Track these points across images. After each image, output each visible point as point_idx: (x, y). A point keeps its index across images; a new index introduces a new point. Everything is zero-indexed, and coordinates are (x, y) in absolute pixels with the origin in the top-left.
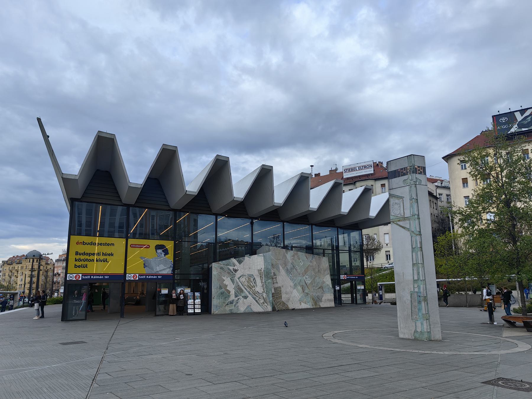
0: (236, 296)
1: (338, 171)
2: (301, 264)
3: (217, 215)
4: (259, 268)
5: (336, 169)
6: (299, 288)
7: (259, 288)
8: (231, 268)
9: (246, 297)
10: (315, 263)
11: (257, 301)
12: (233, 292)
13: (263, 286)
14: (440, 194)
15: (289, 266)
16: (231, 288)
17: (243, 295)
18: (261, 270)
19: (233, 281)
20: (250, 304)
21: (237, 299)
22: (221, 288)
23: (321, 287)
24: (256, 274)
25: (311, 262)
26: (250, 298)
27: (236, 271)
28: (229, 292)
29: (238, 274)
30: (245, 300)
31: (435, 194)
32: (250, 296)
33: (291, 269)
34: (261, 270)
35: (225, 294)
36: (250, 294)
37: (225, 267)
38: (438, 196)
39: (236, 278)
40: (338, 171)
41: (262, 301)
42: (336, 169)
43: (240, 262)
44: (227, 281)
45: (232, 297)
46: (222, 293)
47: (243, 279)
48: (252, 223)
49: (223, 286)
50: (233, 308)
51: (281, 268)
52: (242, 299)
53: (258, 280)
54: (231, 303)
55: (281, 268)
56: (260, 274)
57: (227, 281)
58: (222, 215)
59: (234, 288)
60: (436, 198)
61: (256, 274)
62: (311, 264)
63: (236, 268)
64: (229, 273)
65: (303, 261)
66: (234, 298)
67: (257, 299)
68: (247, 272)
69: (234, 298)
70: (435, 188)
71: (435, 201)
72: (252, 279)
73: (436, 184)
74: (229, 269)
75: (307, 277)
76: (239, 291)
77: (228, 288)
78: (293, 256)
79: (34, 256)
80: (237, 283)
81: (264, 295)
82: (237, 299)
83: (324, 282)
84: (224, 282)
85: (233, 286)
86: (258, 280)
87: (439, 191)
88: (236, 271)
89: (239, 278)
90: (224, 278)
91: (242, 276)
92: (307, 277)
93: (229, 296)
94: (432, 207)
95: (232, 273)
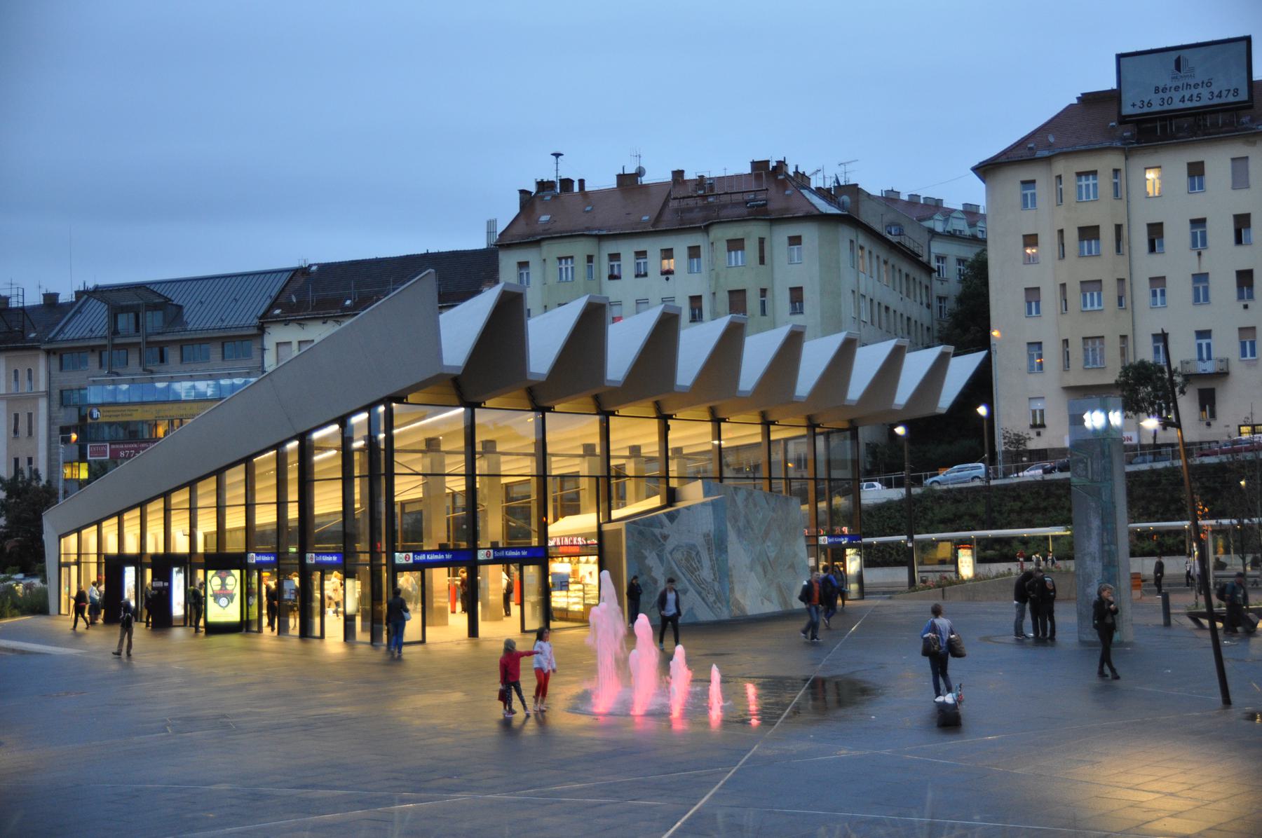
1: (645, 180)
2: (760, 517)
5: (640, 172)
6: (759, 569)
8: (657, 531)
13: (713, 568)
14: (941, 258)
15: (741, 524)
19: (660, 558)
23: (792, 566)
24: (699, 541)
25: (774, 510)
28: (655, 581)
29: (670, 545)
31: (925, 259)
32: (691, 589)
38: (934, 264)
40: (645, 180)
41: (712, 599)
42: (640, 172)
47: (678, 555)
56: (708, 542)
60: (928, 269)
61: (699, 541)
63: (665, 531)
67: (704, 593)
71: (924, 279)
72: (694, 554)
74: (654, 535)
77: (653, 574)
78: (746, 499)
85: (662, 570)
87: (938, 248)
88: (665, 537)
90: (646, 553)
94: (918, 299)
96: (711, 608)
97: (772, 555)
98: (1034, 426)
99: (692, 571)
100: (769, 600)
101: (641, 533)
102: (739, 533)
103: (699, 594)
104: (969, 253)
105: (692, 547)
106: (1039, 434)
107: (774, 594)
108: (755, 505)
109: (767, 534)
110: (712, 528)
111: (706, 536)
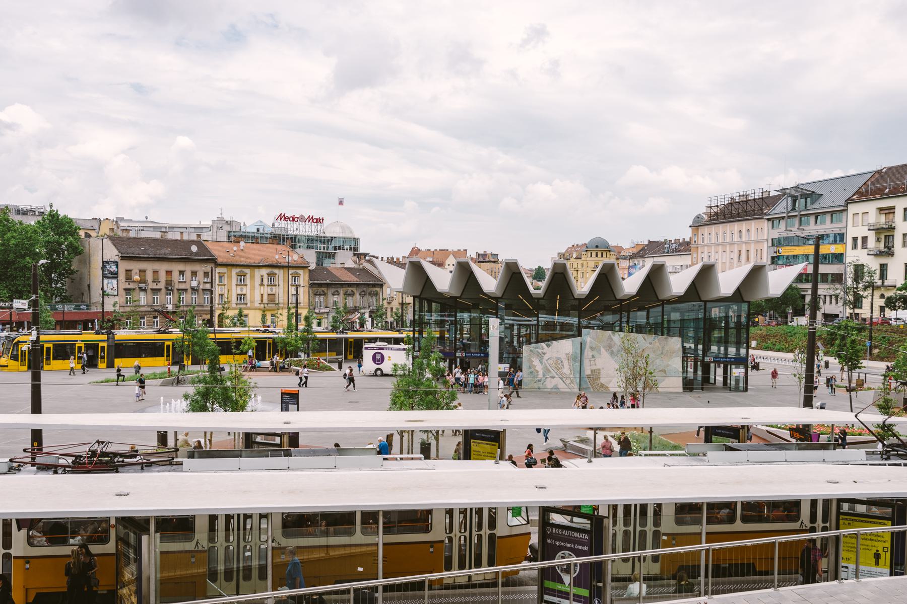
7: (566, 370)
8: (540, 351)
16: (539, 368)
19: (541, 362)
22: (530, 368)
24: (563, 357)
25: (651, 343)
29: (546, 357)
35: (533, 373)
37: (535, 350)
39: (544, 360)
43: (548, 346)
44: (536, 362)
45: (541, 375)
47: (550, 361)
51: (603, 350)
53: (566, 363)
54: (540, 381)
55: (603, 350)
57: (536, 362)
61: (563, 357)
68: (555, 355)
76: (547, 370)
79: (597, 247)
83: (668, 365)
86: (566, 363)
91: (550, 358)
95: (541, 356)
105: (559, 359)
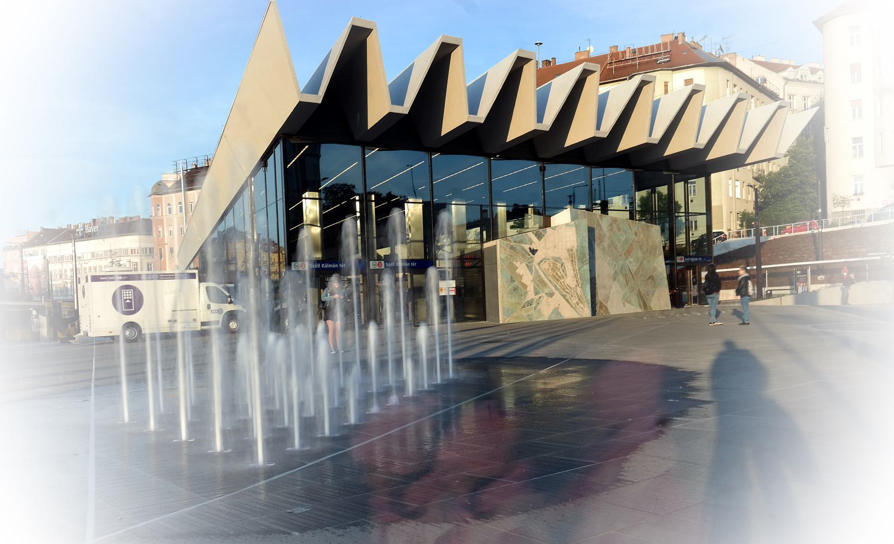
0: (536, 294)
2: (623, 239)
3: (431, 151)
4: (569, 247)
6: (621, 278)
7: (570, 280)
8: (527, 247)
9: (551, 295)
10: (642, 235)
11: (567, 301)
12: (531, 288)
13: (576, 276)
16: (528, 279)
17: (547, 291)
18: (572, 250)
19: (530, 268)
20: (557, 305)
21: (537, 297)
23: (651, 277)
26: (557, 295)
27: (534, 252)
28: (525, 287)
29: (538, 257)
30: (550, 299)
32: (557, 293)
33: (609, 247)
34: (572, 250)
35: (518, 289)
36: (557, 289)
37: (518, 246)
39: (535, 263)
41: (575, 301)
45: (531, 295)
46: (515, 289)
47: (545, 266)
48: (543, 169)
49: (514, 278)
50: (533, 312)
52: (546, 297)
53: (569, 267)
54: (530, 303)
56: (571, 256)
58: (372, 145)
59: (533, 281)
61: (564, 255)
62: (636, 238)
63: (534, 247)
64: (523, 256)
65: (625, 232)
66: (533, 296)
67: (568, 297)
68: (551, 253)
69: (533, 296)
70: (783, 82)
72: (559, 265)
73: (784, 74)
74: (523, 249)
75: (631, 260)
76: (540, 283)
77: (523, 281)
78: (611, 225)
80: (537, 271)
81: (579, 290)
82: (537, 297)
83: (655, 269)
84: (517, 271)
85: (531, 277)
86: (569, 267)
87: (791, 88)
88: (534, 252)
89: (539, 264)
90: (517, 264)
92: (631, 260)
93: (526, 293)
96: (574, 308)
97: (634, 269)
98: (855, 194)
99: (557, 278)
100: (630, 302)
101: (512, 248)
102: (604, 249)
103: (564, 296)
104: (814, 93)
105: (557, 260)
106: (859, 200)
107: (634, 299)
108: (619, 230)
109: (628, 253)
110: (576, 245)
111: (570, 250)
